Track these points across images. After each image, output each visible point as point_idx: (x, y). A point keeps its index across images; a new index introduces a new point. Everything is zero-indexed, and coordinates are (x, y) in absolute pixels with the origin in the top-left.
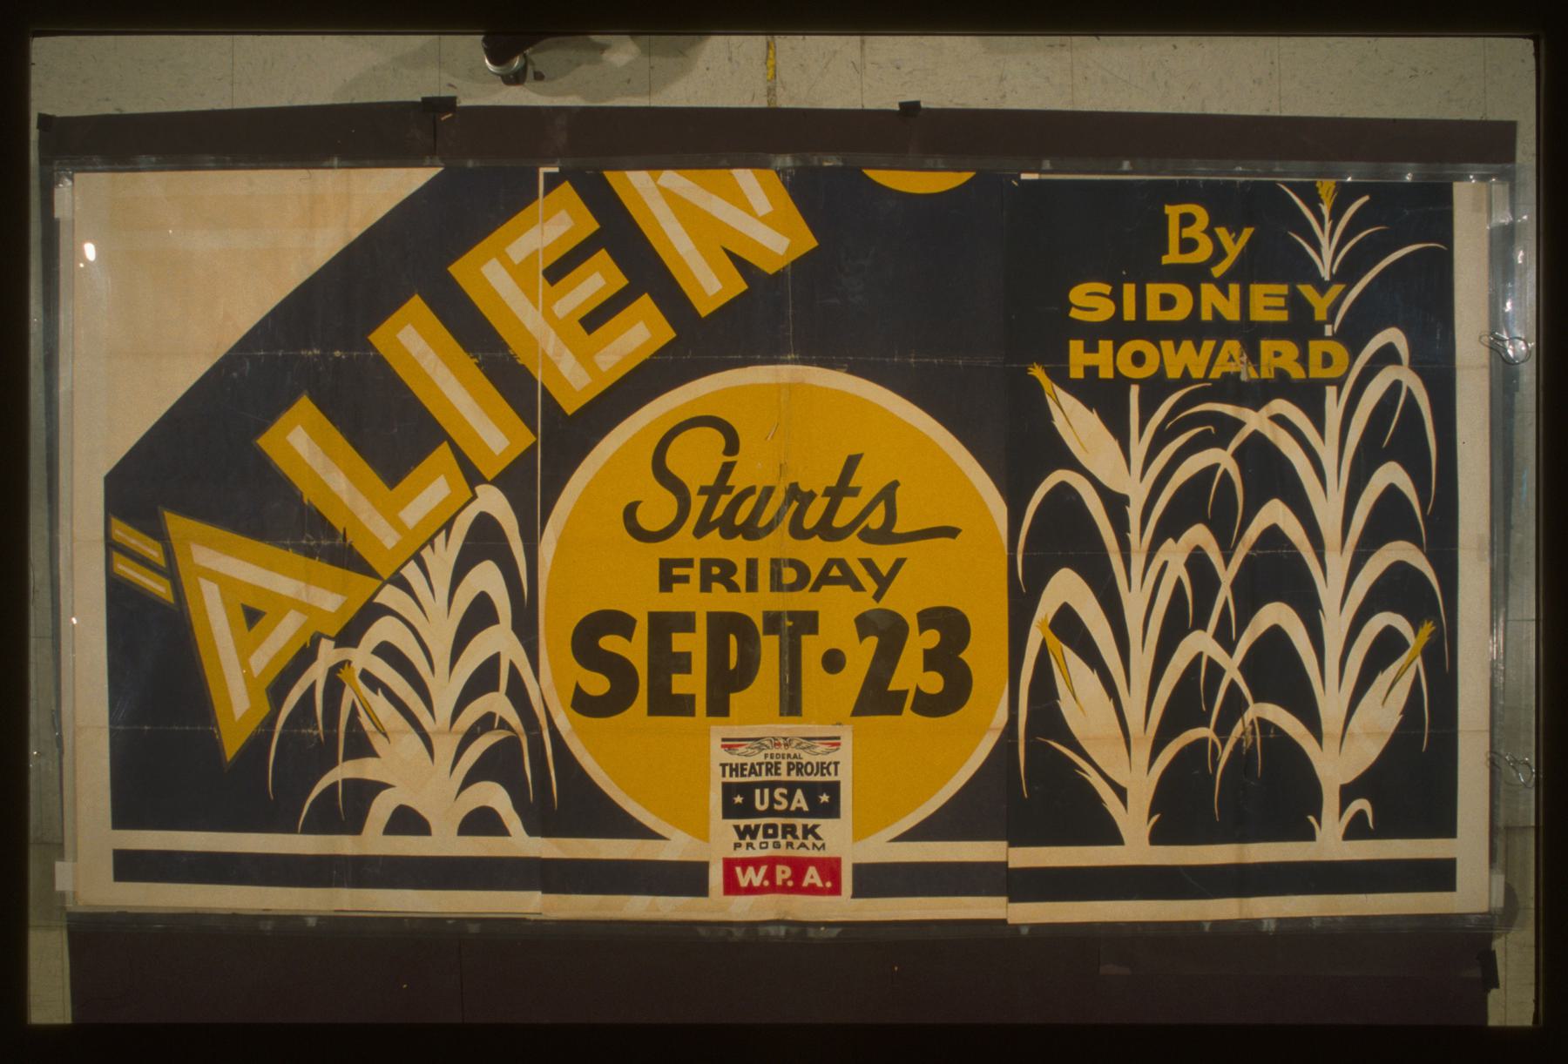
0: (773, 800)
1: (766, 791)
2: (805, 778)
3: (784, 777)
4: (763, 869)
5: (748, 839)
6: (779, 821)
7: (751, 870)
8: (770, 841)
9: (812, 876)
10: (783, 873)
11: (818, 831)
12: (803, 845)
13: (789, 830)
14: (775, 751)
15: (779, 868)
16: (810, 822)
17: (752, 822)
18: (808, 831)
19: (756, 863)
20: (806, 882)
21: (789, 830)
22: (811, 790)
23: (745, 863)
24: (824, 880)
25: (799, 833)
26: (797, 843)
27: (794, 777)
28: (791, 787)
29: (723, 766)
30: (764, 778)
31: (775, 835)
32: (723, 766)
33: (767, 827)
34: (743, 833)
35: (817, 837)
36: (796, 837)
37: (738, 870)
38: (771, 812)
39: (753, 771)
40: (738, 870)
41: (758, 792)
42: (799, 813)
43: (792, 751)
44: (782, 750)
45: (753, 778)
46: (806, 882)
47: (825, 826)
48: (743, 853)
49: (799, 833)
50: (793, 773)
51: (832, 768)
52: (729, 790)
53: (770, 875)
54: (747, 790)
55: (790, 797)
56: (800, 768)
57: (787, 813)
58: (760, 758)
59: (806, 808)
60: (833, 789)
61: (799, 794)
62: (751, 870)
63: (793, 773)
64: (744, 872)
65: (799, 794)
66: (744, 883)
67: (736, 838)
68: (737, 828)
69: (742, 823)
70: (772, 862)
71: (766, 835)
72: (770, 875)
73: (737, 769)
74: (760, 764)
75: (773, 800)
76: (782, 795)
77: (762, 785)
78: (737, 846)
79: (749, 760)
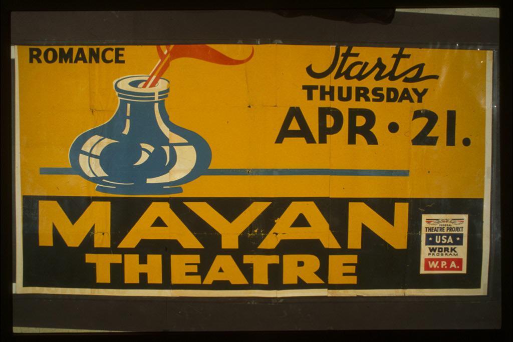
0: (441, 240)
1: (440, 237)
3: (445, 232)
4: (437, 262)
5: (433, 252)
6: (443, 247)
7: (433, 262)
8: (440, 253)
9: (453, 264)
10: (444, 264)
11: (456, 250)
12: (451, 254)
14: (443, 224)
15: (442, 262)
16: (453, 247)
17: (435, 247)
18: (452, 250)
19: (435, 260)
21: (446, 249)
22: (454, 236)
23: (432, 260)
24: (457, 266)
25: (450, 250)
26: (448, 254)
27: (449, 232)
28: (448, 235)
29: (426, 228)
31: (442, 251)
32: (426, 228)
33: (439, 248)
34: (431, 250)
35: (455, 252)
36: (448, 252)
37: (429, 262)
38: (441, 244)
39: (435, 230)
40: (429, 262)
41: (437, 237)
42: (450, 244)
43: (448, 224)
45: (435, 232)
48: (431, 257)
49: (450, 250)
50: (449, 231)
51: (461, 229)
52: (428, 236)
53: (440, 264)
54: (433, 236)
55: (447, 239)
56: (451, 229)
58: (438, 226)
60: (461, 236)
61: (450, 238)
62: (433, 262)
63: (449, 231)
64: (431, 263)
65: (450, 238)
66: (431, 266)
67: (429, 251)
68: (430, 248)
69: (431, 247)
70: (440, 260)
71: (439, 251)
72: (440, 264)
73: (431, 229)
74: (438, 228)
76: (445, 238)
79: (434, 226)
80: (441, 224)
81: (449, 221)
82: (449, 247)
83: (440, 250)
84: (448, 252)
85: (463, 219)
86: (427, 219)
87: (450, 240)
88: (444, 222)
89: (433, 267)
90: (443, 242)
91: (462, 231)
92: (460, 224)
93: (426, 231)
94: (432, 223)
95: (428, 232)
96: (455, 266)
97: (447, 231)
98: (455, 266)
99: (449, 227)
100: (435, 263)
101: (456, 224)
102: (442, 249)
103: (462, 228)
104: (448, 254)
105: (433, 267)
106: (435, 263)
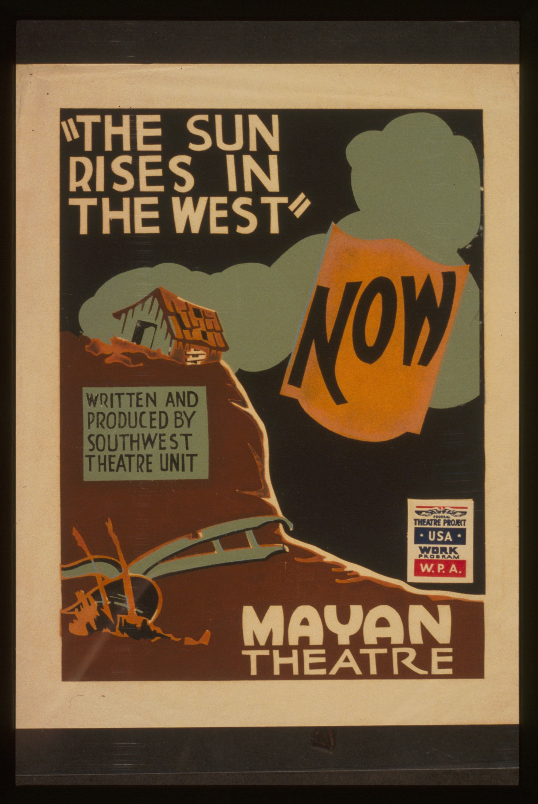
0: (437, 537)
1: (434, 532)
2: (451, 527)
3: (442, 526)
4: (432, 565)
5: (425, 553)
6: (439, 546)
7: (426, 565)
8: (435, 555)
9: (453, 568)
10: (441, 567)
11: (456, 550)
12: (449, 557)
13: (444, 550)
14: (438, 515)
15: (439, 565)
16: (453, 546)
17: (427, 546)
18: (452, 550)
19: (429, 562)
20: (450, 572)
21: (444, 550)
22: (454, 532)
23: (424, 562)
24: (458, 570)
25: (448, 551)
26: (447, 556)
27: (446, 526)
28: (445, 530)
29: (415, 520)
30: (433, 526)
31: (437, 552)
32: (415, 520)
33: (434, 548)
34: (423, 550)
35: (456, 553)
36: (446, 553)
37: (421, 565)
38: (436, 542)
39: (428, 523)
40: (421, 565)
41: (430, 533)
42: (448, 542)
44: (441, 514)
45: (428, 526)
46: (451, 571)
47: (460, 548)
48: (423, 558)
49: (448, 551)
50: (446, 524)
51: (463, 523)
52: (417, 531)
53: (435, 568)
54: (426, 531)
55: (444, 535)
56: (449, 522)
57: (443, 542)
58: (431, 517)
59: (451, 540)
60: (463, 532)
61: (448, 534)
62: (426, 565)
63: (446, 524)
64: (424, 566)
65: (448, 534)
66: (423, 570)
67: (420, 553)
68: (420, 548)
69: (423, 546)
70: (436, 562)
71: (433, 552)
72: (435, 568)
73: (422, 522)
74: (432, 520)
75: (437, 537)
76: (441, 534)
77: (432, 530)
79: (427, 518)
80: (435, 515)
81: (447, 511)
82: (448, 546)
84: (446, 553)
86: (418, 507)
88: (439, 512)
89: (426, 570)
90: (438, 540)
91: (464, 525)
92: (461, 516)
93: (416, 524)
94: (424, 513)
95: (417, 526)
97: (444, 525)
99: (447, 519)
100: (429, 566)
101: (457, 516)
102: (437, 548)
103: (465, 521)
104: (447, 556)
105: (426, 570)
106: (429, 566)
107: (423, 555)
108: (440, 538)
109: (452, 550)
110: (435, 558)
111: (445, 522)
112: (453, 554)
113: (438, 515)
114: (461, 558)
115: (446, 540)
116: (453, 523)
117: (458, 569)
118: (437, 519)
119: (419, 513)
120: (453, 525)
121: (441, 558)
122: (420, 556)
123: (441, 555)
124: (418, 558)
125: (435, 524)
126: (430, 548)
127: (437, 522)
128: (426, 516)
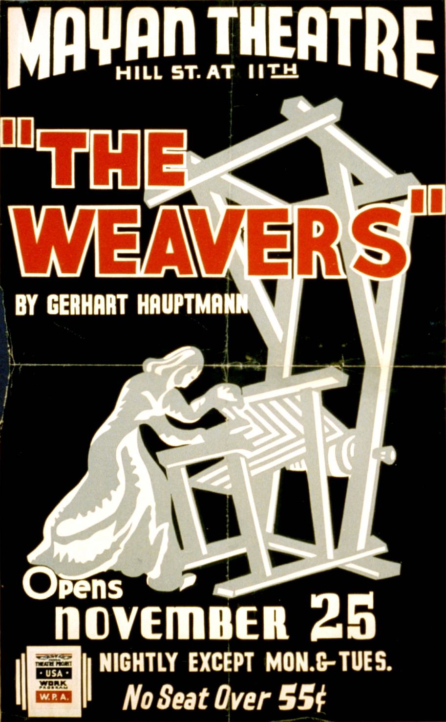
0: (52, 674)
1: (50, 671)
2: (62, 667)
3: (55, 666)
4: (48, 695)
6: (54, 680)
7: (44, 695)
8: (51, 687)
9: (63, 697)
10: (54, 696)
11: (66, 683)
12: (61, 687)
13: (57, 683)
14: (52, 658)
15: (53, 695)
16: (63, 680)
17: (45, 680)
18: (63, 683)
19: (46, 693)
20: (62, 698)
21: (57, 683)
22: (64, 670)
23: (43, 693)
24: (67, 698)
25: (60, 683)
26: (59, 687)
27: (58, 666)
28: (57, 669)
30: (49, 667)
31: (52, 684)
32: (37, 663)
33: (50, 682)
34: (43, 683)
35: (65, 685)
36: (58, 685)
37: (41, 695)
38: (51, 677)
40: (41, 695)
41: (47, 671)
42: (60, 678)
43: (57, 658)
44: (54, 658)
45: (45, 667)
46: (62, 698)
47: (67, 681)
48: (42, 689)
49: (60, 683)
50: (58, 665)
51: (69, 664)
52: (38, 670)
53: (50, 697)
54: (44, 670)
55: (57, 672)
56: (60, 664)
57: (56, 678)
58: (47, 660)
59: (61, 675)
60: (70, 670)
61: (60, 672)
62: (44, 695)
63: (58, 665)
64: (42, 695)
65: (60, 672)
66: (42, 698)
68: (40, 682)
69: (42, 680)
70: (51, 693)
71: (50, 685)
72: (50, 697)
73: (41, 664)
74: (48, 662)
75: (52, 674)
76: (54, 672)
77: (48, 669)
78: (41, 687)
79: (44, 661)
81: (58, 656)
82: (60, 680)
83: (51, 683)
84: (58, 685)
85: (71, 654)
87: (60, 674)
88: (53, 657)
89: (44, 699)
90: (53, 676)
91: (71, 665)
92: (68, 659)
93: (37, 665)
94: (42, 658)
96: (65, 698)
97: (57, 665)
98: (65, 698)
99: (58, 661)
100: (46, 695)
101: (65, 659)
102: (52, 682)
103: (71, 662)
104: (59, 687)
105: (44, 699)
106: (46, 695)
107: (43, 686)
108: (53, 675)
109: (63, 683)
110: (51, 690)
111: (57, 663)
112: (63, 686)
113: (52, 658)
114: (68, 690)
115: (58, 676)
116: (63, 664)
117: (67, 697)
118: (52, 662)
119: (39, 658)
120: (63, 665)
121: (55, 689)
122: (41, 687)
123: (55, 687)
124: (38, 689)
125: (50, 665)
126: (47, 682)
127: (51, 664)
128: (44, 659)
